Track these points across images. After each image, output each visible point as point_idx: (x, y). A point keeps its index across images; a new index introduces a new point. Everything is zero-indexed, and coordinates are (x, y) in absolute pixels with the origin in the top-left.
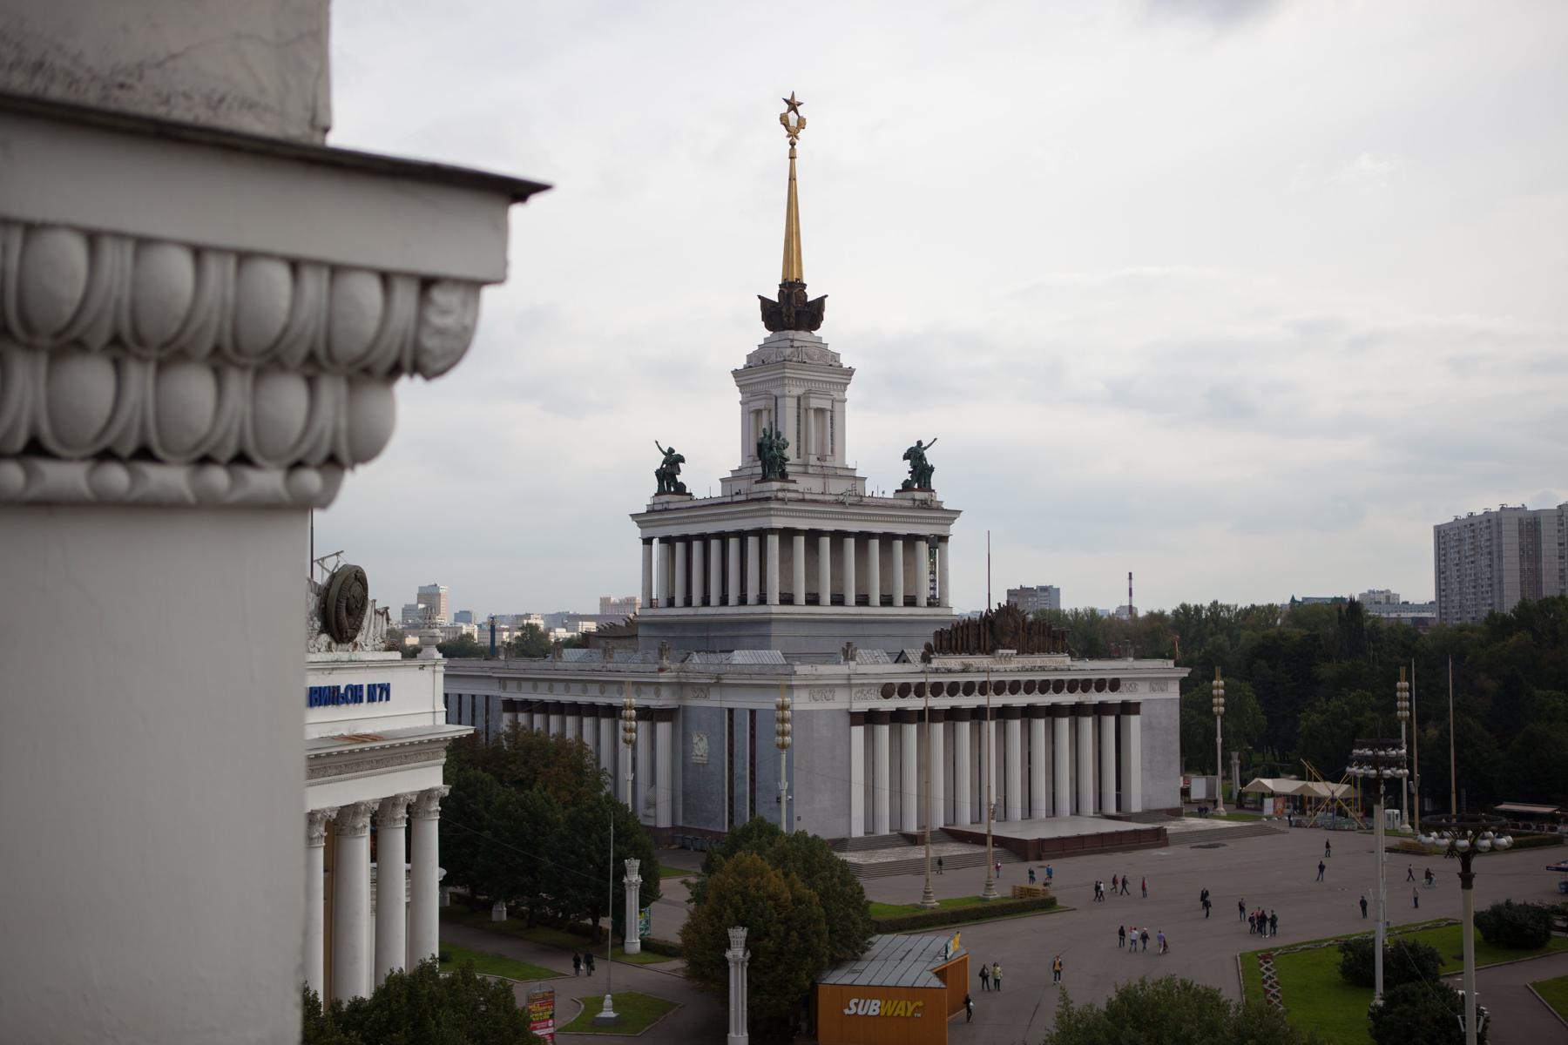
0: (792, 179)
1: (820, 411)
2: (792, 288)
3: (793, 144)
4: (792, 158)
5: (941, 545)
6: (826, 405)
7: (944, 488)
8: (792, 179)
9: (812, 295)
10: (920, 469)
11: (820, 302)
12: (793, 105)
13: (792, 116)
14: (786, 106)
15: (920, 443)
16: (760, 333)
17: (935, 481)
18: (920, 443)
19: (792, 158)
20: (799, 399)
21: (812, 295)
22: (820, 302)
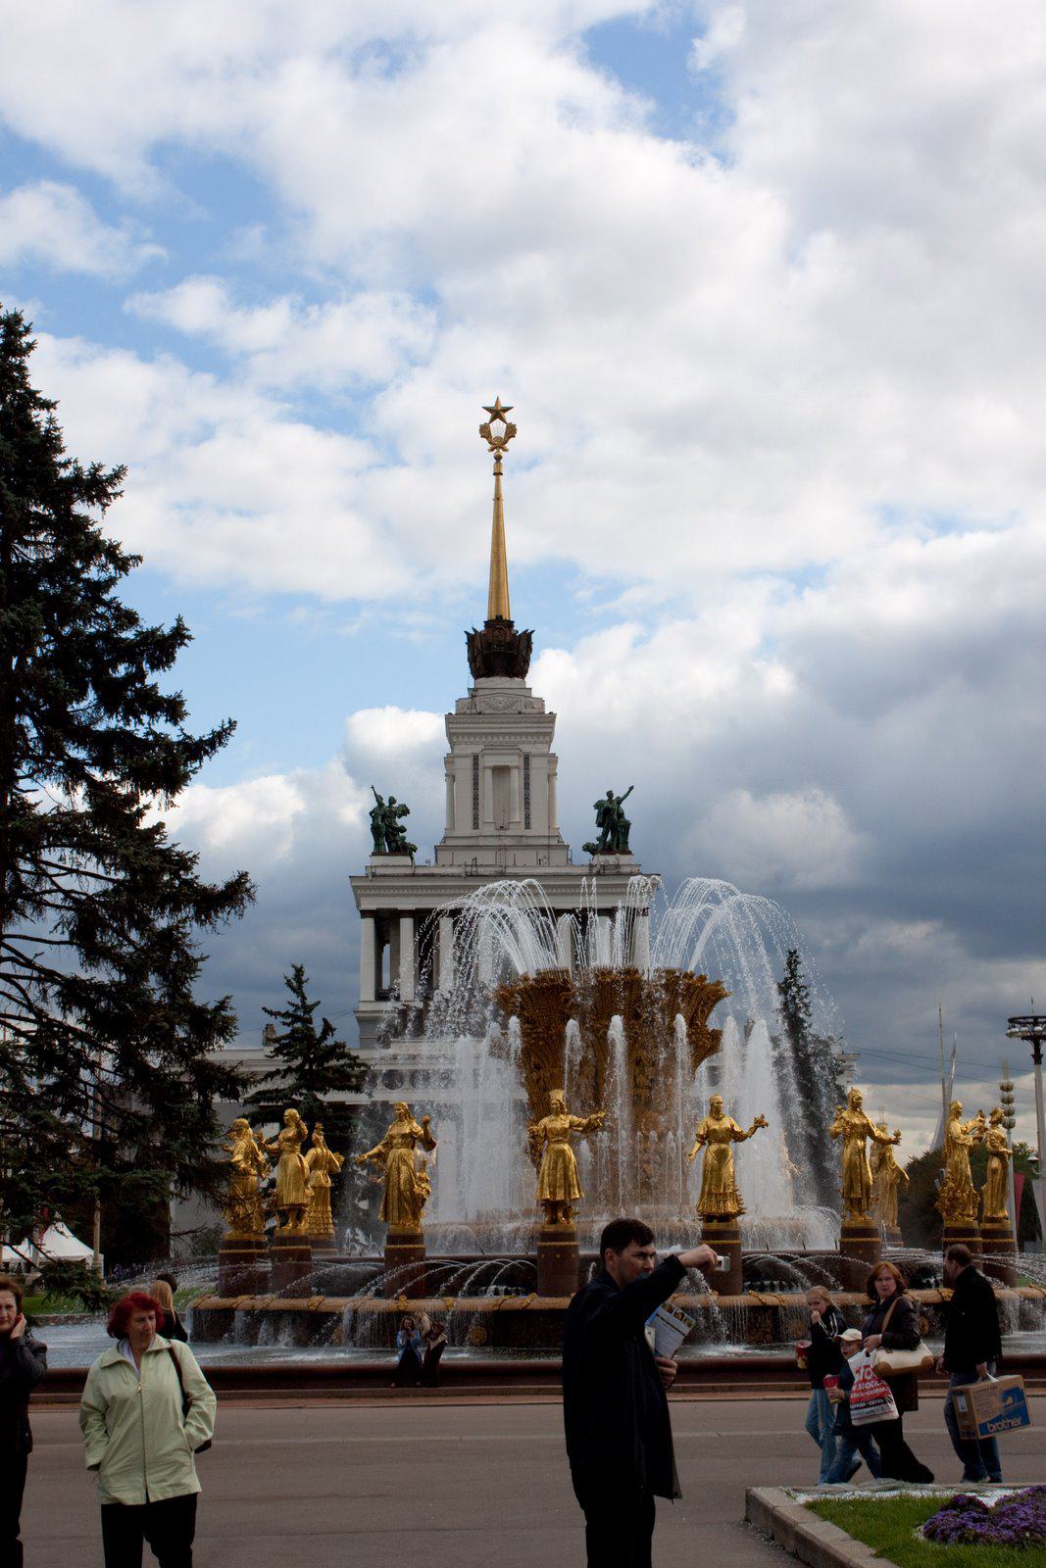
0: (498, 499)
1: (501, 771)
2: (499, 624)
3: (498, 458)
4: (498, 474)
6: (513, 761)
8: (498, 499)
9: (519, 628)
12: (497, 413)
13: (498, 428)
14: (489, 415)
15: (610, 794)
17: (634, 839)
18: (610, 794)
19: (498, 474)
20: (476, 758)
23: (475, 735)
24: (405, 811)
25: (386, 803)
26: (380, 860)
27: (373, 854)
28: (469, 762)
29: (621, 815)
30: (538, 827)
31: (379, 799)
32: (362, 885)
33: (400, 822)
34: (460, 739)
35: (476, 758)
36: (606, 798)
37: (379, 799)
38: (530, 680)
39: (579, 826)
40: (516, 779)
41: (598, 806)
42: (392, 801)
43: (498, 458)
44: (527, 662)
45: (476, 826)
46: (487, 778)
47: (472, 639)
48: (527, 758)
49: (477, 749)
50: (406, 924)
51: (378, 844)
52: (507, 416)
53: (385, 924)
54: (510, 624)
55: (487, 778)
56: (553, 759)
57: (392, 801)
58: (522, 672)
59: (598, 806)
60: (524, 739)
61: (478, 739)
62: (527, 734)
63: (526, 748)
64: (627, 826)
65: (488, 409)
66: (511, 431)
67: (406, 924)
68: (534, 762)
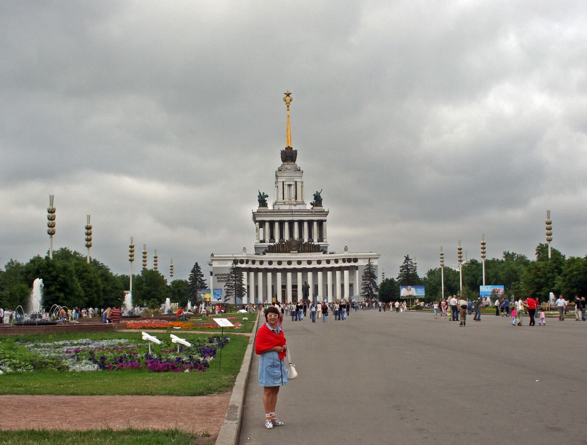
1: (290, 185)
2: (289, 149)
3: (288, 106)
5: (324, 223)
6: (292, 183)
7: (325, 207)
10: (318, 200)
11: (296, 151)
12: (288, 95)
14: (286, 96)
15: (317, 192)
16: (280, 163)
18: (317, 192)
20: (283, 182)
21: (294, 149)
22: (296, 151)
24: (267, 196)
25: (262, 194)
26: (262, 208)
28: (282, 183)
29: (320, 197)
30: (299, 199)
31: (260, 193)
33: (266, 199)
35: (283, 182)
36: (316, 193)
37: (260, 193)
38: (297, 162)
39: (309, 200)
40: (293, 188)
41: (314, 195)
42: (264, 193)
43: (288, 106)
44: (296, 158)
45: (283, 199)
46: (286, 187)
47: (283, 152)
48: (296, 182)
49: (283, 180)
50: (267, 225)
51: (260, 204)
52: (290, 95)
54: (292, 148)
55: (286, 187)
56: (302, 182)
57: (264, 193)
58: (295, 161)
59: (314, 195)
63: (296, 180)
65: (286, 94)
66: (291, 100)
67: (267, 225)
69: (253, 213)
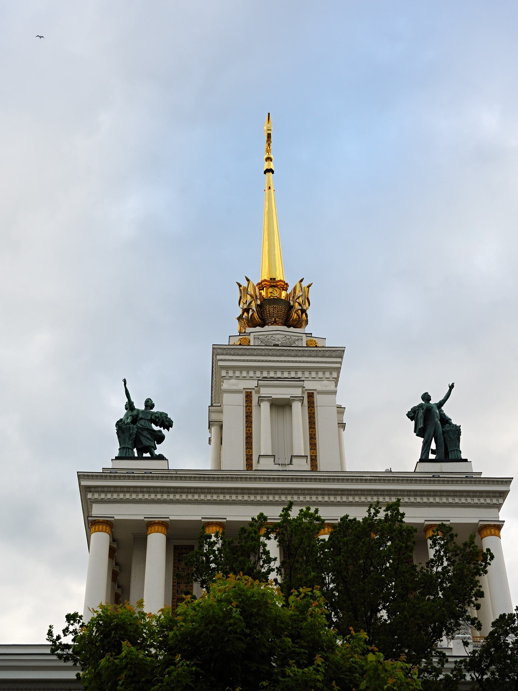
23: (248, 369)
27: (117, 458)
29: (445, 420)
32: (92, 488)
34: (231, 374)
41: (412, 415)
48: (311, 396)
53: (123, 551)
59: (412, 415)
60: (307, 374)
61: (251, 374)
62: (310, 370)
63: (309, 385)
64: (457, 431)
67: (156, 544)
68: (318, 399)
69: (81, 476)
